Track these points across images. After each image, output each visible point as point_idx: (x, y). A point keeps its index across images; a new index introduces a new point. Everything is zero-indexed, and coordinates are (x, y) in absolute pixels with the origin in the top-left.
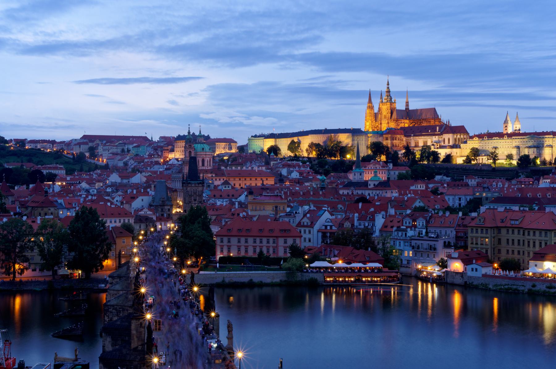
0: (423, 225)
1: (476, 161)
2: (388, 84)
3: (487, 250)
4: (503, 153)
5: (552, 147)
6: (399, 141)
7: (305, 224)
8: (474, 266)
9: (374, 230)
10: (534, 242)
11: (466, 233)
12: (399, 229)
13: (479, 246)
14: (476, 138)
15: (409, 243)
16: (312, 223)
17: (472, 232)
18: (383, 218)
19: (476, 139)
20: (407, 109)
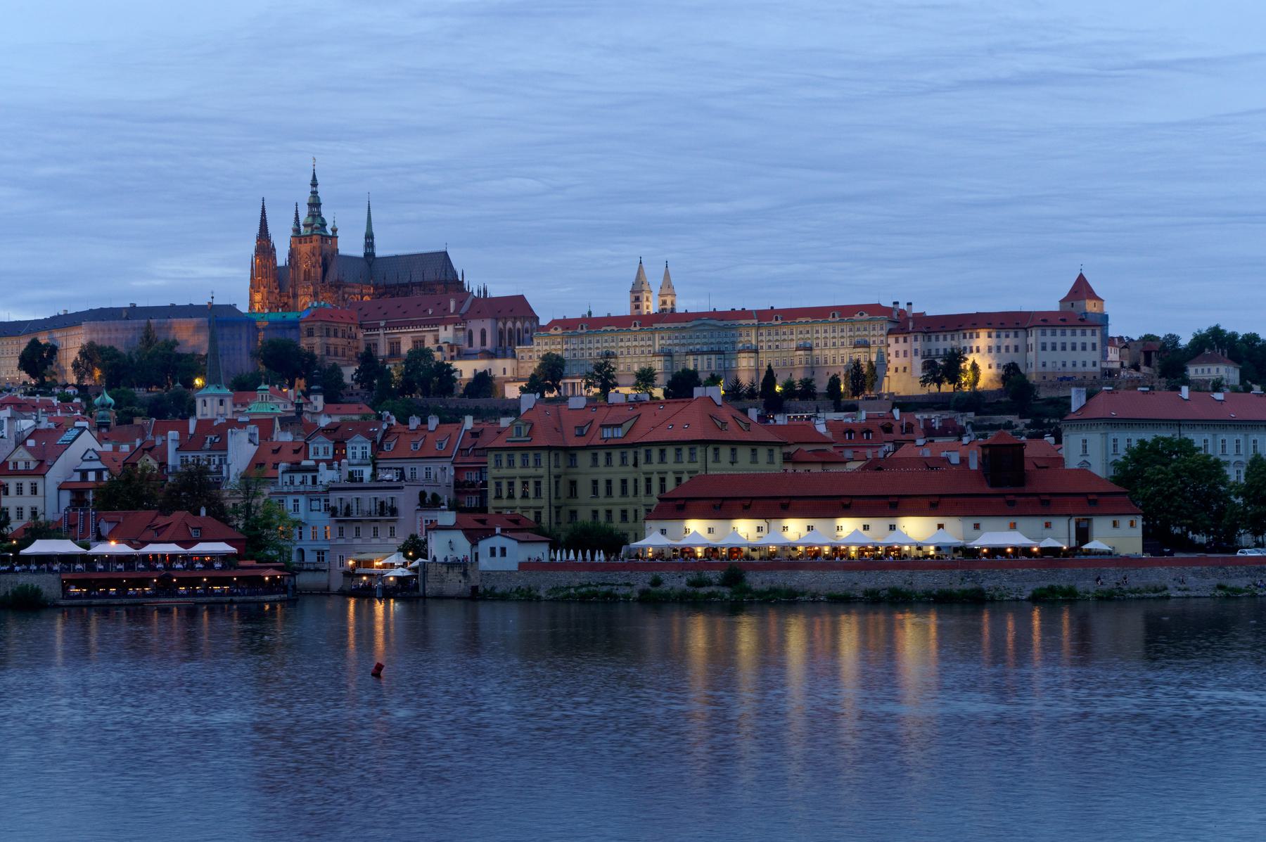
0: (364, 455)
1: (556, 393)
2: (314, 183)
3: (540, 513)
4: (629, 369)
5: (756, 351)
6: (345, 341)
7: (21, 466)
8: (498, 541)
9: (225, 474)
11: (482, 470)
12: (295, 468)
13: (518, 502)
14: (556, 329)
15: (322, 500)
16: (42, 462)
17: (498, 464)
18: (250, 441)
19: (555, 332)
20: (370, 255)
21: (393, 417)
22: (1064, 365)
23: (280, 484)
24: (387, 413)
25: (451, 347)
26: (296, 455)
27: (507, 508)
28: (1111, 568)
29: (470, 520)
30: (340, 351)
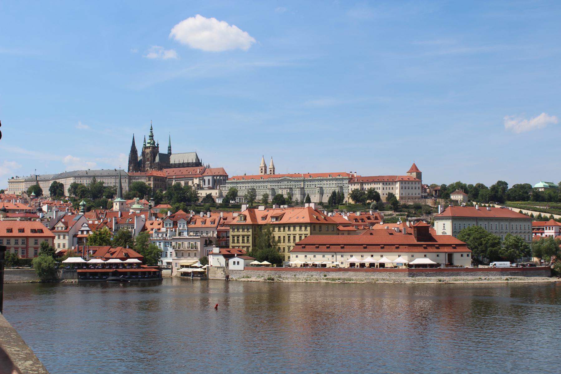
2: (151, 129)
7: (60, 229)
8: (236, 259)
10: (294, 237)
11: (227, 232)
14: (234, 179)
15: (170, 243)
17: (234, 230)
21: (194, 212)
22: (409, 194)
23: (154, 236)
24: (192, 211)
25: (198, 185)
26: (159, 226)
27: (237, 246)
28: (462, 272)
29: (224, 251)
30: (160, 186)
